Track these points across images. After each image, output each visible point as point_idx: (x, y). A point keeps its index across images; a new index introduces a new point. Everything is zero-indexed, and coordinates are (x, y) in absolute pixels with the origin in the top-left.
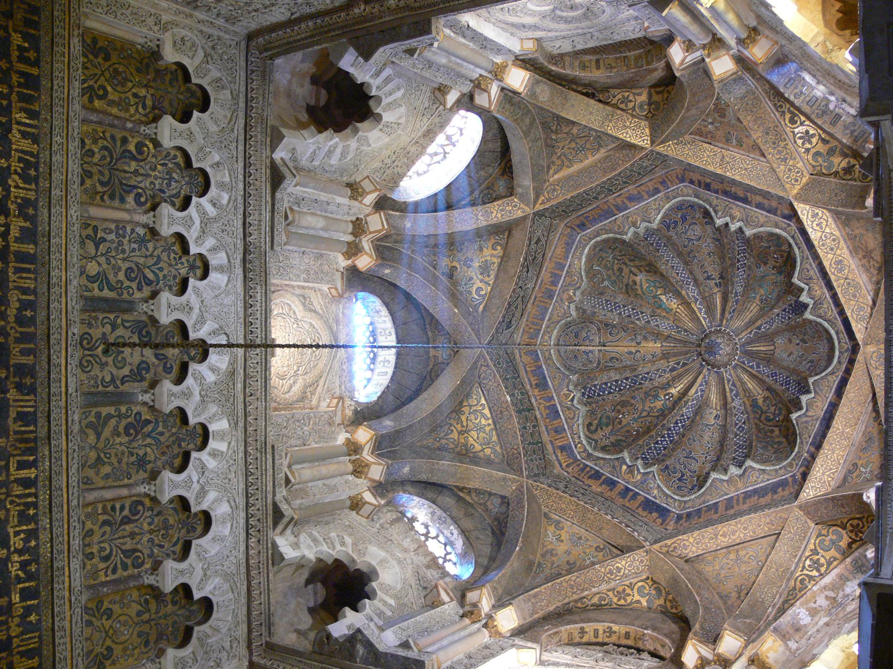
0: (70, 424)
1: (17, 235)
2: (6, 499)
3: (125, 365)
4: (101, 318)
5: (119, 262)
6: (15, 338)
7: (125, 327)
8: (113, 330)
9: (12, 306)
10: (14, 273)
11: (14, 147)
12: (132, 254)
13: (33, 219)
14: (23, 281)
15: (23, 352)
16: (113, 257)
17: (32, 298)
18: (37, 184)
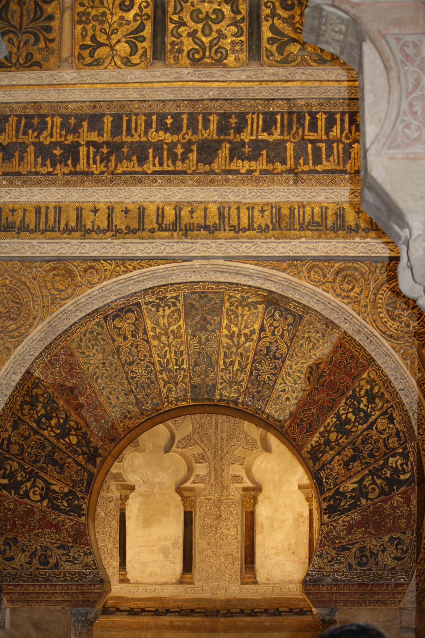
0: (276, 78)
1: (96, 133)
2: (343, 143)
3: (220, 10)
4: (173, 39)
5: (115, 18)
6: (192, 135)
7: (182, 10)
8: (184, 24)
9: (163, 138)
10: (132, 136)
11: (14, 140)
12: (106, 5)
13: (80, 119)
14: (139, 127)
15: (206, 126)
16: (110, 27)
17: (154, 118)
18: (46, 116)
